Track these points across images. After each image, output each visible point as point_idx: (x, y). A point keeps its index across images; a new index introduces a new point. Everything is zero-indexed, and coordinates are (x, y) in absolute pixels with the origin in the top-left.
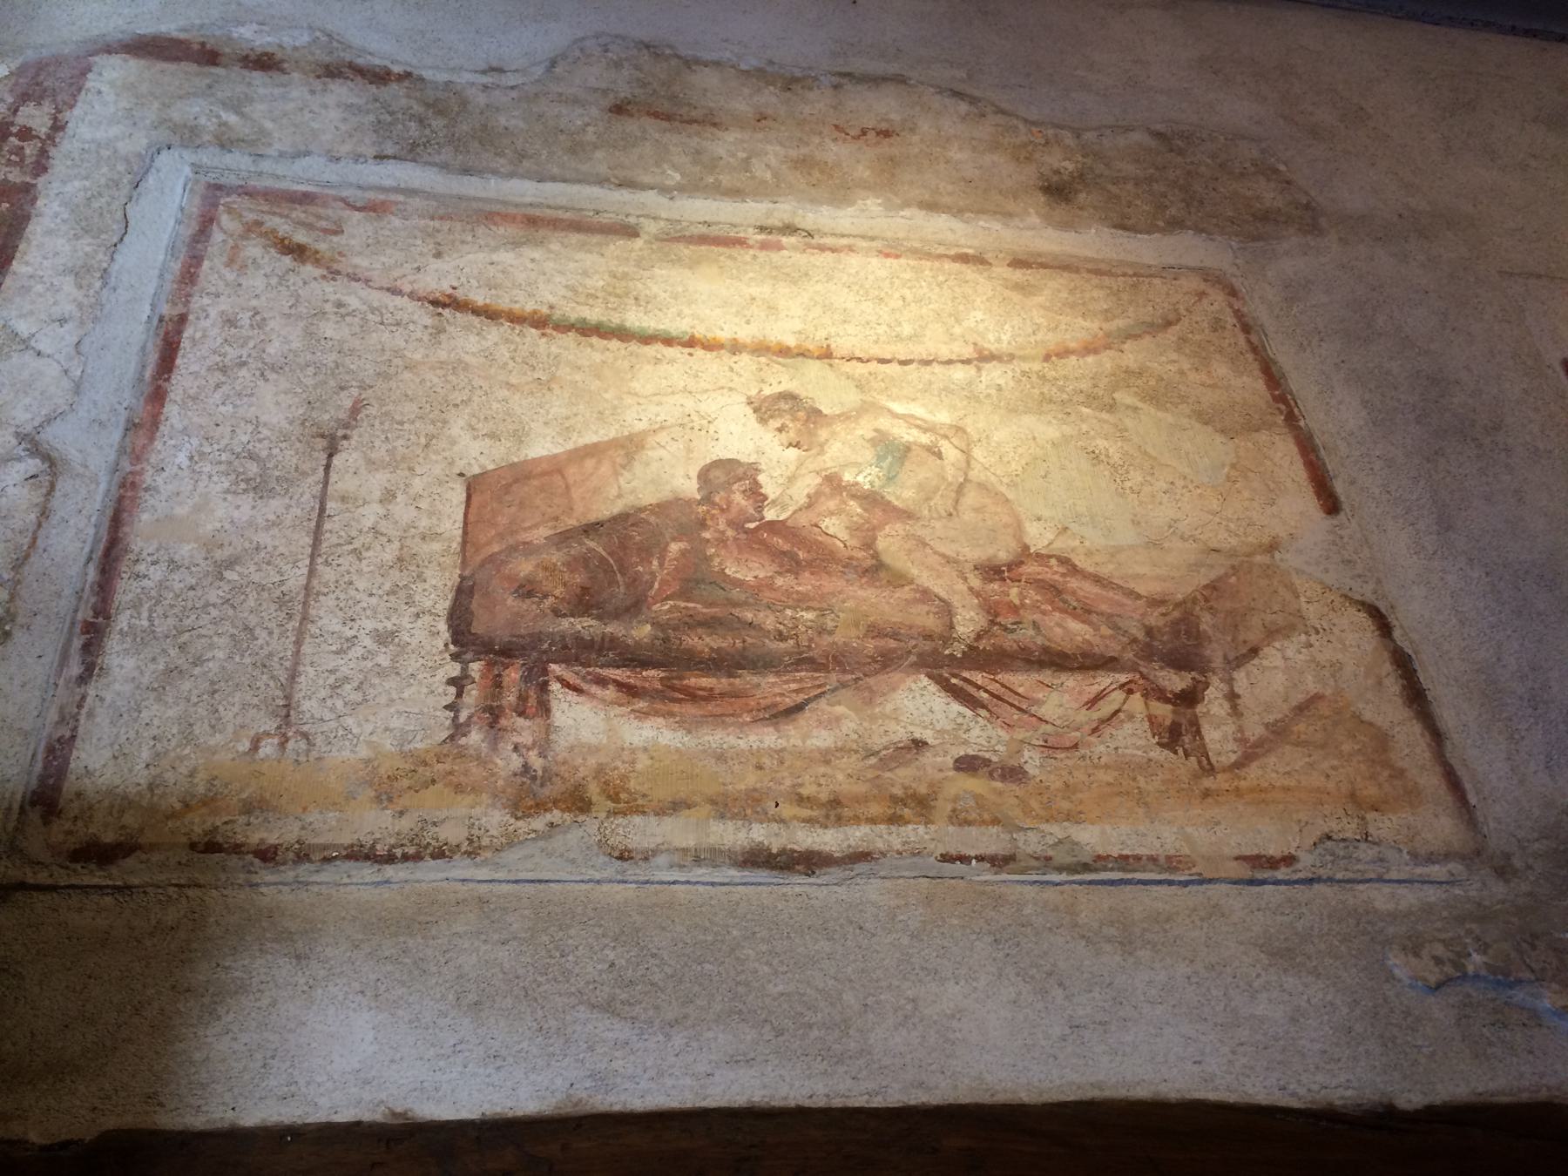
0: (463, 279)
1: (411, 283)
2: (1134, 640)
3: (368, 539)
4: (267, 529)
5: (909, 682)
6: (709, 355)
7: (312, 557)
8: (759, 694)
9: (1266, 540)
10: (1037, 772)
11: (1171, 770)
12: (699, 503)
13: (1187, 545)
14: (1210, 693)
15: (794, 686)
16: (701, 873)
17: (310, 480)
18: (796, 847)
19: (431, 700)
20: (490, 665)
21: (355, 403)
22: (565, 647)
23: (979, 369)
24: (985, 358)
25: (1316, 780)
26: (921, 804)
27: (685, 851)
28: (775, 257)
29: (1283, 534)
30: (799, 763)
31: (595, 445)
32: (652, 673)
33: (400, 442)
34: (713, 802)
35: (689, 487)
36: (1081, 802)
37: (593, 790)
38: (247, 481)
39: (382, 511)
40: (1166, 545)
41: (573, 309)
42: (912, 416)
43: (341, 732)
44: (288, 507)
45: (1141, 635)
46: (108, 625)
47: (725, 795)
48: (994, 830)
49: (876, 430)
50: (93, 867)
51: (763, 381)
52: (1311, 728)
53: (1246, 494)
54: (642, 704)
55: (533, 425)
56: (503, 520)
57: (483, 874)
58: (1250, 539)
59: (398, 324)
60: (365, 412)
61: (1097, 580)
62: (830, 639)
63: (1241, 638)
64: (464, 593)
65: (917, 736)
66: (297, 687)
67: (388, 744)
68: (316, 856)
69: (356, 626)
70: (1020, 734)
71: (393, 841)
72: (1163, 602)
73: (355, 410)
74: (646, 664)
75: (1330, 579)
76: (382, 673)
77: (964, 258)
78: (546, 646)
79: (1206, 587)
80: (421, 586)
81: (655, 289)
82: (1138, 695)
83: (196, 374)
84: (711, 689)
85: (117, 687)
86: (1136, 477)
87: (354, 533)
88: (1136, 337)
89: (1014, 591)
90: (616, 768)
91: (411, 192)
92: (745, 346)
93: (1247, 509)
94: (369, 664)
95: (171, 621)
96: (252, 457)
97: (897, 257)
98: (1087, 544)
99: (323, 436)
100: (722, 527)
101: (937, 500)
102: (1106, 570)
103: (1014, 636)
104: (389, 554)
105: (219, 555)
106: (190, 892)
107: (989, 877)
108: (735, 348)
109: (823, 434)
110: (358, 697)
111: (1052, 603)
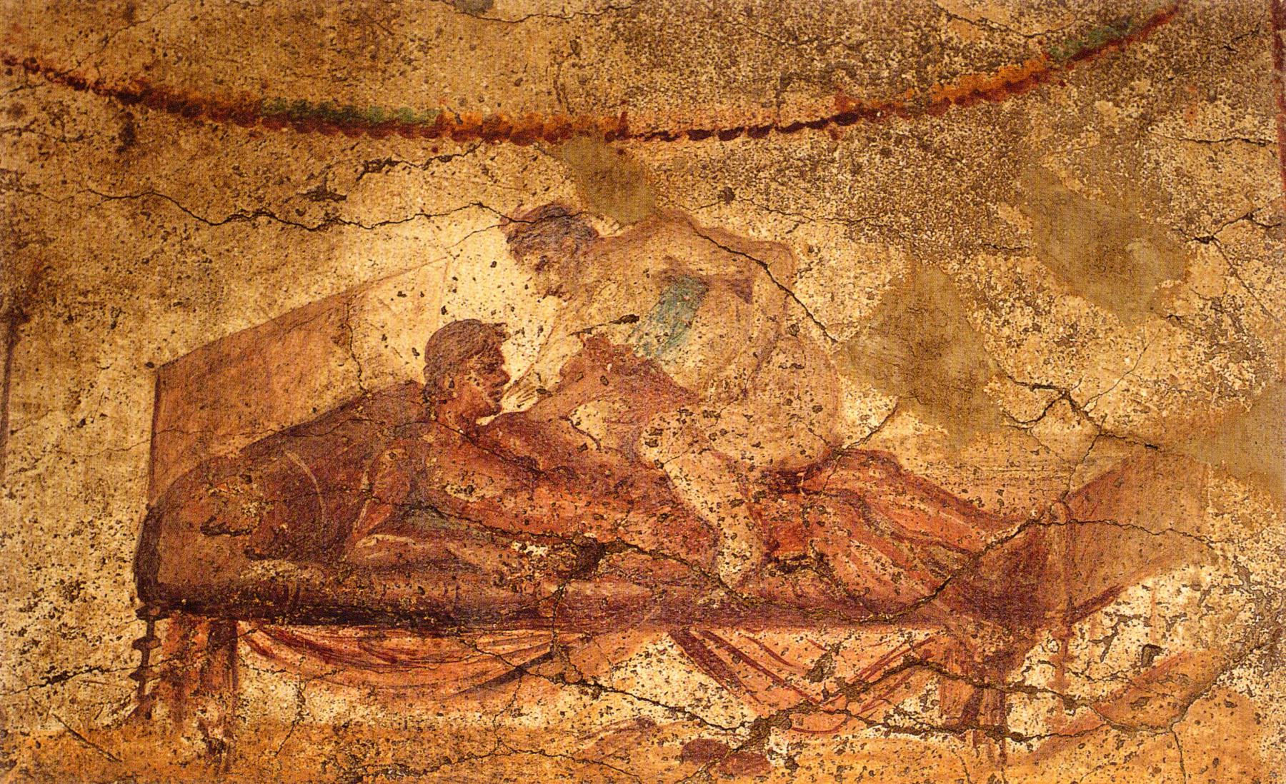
20: (179, 622)
23: (835, 136)
31: (303, 311)
32: (349, 632)
65: (645, 713)
80: (107, 522)
104: (72, 483)
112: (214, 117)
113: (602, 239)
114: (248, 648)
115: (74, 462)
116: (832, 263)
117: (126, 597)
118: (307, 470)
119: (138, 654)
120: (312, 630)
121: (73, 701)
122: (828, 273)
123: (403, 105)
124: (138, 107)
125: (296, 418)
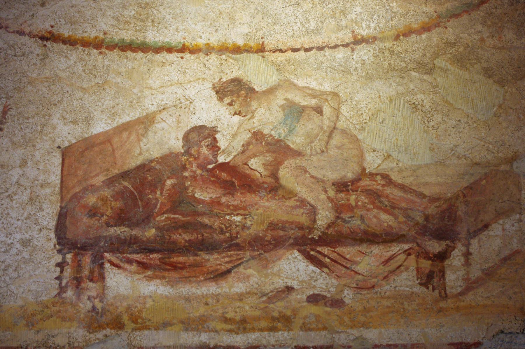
1: (29, 26)
2: (417, 224)
3: (14, 189)
5: (288, 255)
6: (193, 57)
8: (208, 265)
9: (510, 155)
10: (350, 301)
11: (424, 298)
13: (460, 162)
15: (227, 259)
18: (222, 344)
19: (49, 275)
20: (76, 255)
21: (5, 108)
22: (112, 244)
23: (353, 50)
24: (358, 41)
26: (286, 321)
33: (28, 130)
34: (182, 322)
35: (177, 144)
36: (371, 317)
37: (125, 318)
39: (21, 172)
41: (117, 33)
42: (308, 88)
43: (9, 293)
45: (421, 220)
48: (323, 333)
49: (286, 99)
52: (509, 271)
53: (504, 124)
54: (149, 273)
55: (95, 113)
56: (80, 173)
58: (500, 155)
59: (24, 55)
60: (9, 113)
61: (402, 187)
62: (248, 232)
64: (62, 216)
65: (289, 284)
67: (30, 298)
69: (12, 238)
70: (344, 281)
71: (35, 345)
72: (437, 199)
74: (151, 251)
76: (25, 262)
79: (466, 188)
81: (164, 13)
82: (413, 256)
84: (185, 263)
87: (8, 186)
88: (455, 16)
89: (353, 197)
90: (136, 307)
92: (213, 48)
93: (503, 135)
94: (20, 257)
98: (400, 165)
101: (316, 142)
103: (349, 225)
104: (25, 198)
108: (208, 50)
109: (254, 105)
110: (15, 275)
111: (373, 203)
113: (257, 92)
114: (109, 265)
115: (25, 189)
116: (356, 99)
118: (132, 189)
119: (58, 269)
120: (138, 256)
121: (29, 291)
122: (354, 103)
123: (167, 40)
124: (49, 42)
125: (126, 168)
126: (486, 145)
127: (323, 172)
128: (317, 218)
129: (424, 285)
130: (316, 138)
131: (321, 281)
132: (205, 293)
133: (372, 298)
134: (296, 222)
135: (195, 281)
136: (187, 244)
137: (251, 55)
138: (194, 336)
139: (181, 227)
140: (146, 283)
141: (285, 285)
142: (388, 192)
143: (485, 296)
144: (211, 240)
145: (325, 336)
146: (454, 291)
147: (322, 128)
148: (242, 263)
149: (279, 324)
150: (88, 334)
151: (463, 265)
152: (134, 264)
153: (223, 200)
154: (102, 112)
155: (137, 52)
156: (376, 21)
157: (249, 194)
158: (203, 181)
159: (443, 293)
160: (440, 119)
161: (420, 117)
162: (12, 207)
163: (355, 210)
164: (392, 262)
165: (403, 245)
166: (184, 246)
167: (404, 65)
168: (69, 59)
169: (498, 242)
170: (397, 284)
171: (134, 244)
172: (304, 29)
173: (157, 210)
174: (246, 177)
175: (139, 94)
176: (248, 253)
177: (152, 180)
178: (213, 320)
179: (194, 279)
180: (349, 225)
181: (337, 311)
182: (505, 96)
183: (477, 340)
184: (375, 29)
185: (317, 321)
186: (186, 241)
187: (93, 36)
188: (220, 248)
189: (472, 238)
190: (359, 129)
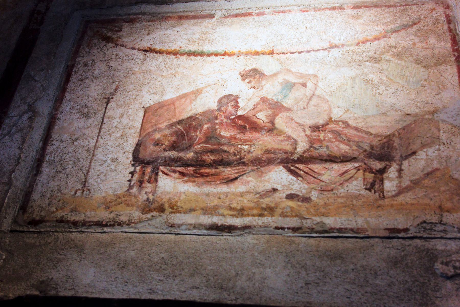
0: (155, 42)
1: (139, 45)
2: (365, 151)
3: (113, 130)
4: (87, 128)
6: (230, 58)
7: (98, 136)
8: (224, 174)
9: (432, 109)
11: (367, 198)
12: (216, 111)
13: (397, 113)
14: (392, 169)
15: (236, 171)
16: (195, 231)
17: (101, 113)
18: (226, 224)
19: (124, 179)
21: (117, 86)
22: (165, 161)
23: (329, 52)
25: (427, 201)
26: (271, 210)
27: (191, 224)
28: (261, 17)
29: (440, 106)
30: (233, 197)
32: (191, 168)
33: (128, 98)
35: (214, 105)
36: (330, 209)
37: (166, 205)
38: (84, 114)
39: (119, 121)
40: (388, 114)
42: (298, 73)
43: (98, 189)
44: (94, 121)
45: (367, 148)
46: (44, 159)
47: (207, 207)
49: (284, 79)
50: (33, 226)
51: (246, 65)
52: (430, 182)
53: (428, 91)
54: (186, 179)
55: (168, 89)
56: (153, 121)
57: (132, 230)
58: (425, 109)
60: (119, 89)
61: (356, 129)
62: (251, 155)
63: (410, 148)
64: (138, 145)
65: (275, 187)
66: (88, 175)
67: (110, 192)
68: (87, 225)
70: (312, 186)
71: (108, 220)
72: (381, 136)
73: (116, 89)
74: (189, 165)
75: (455, 123)
77: (334, 8)
78: (159, 161)
80: (126, 143)
82: (361, 171)
83: (74, 83)
84: (209, 173)
85: (44, 177)
86: (382, 88)
87: (110, 128)
89: (323, 134)
90: (174, 199)
91: (144, 14)
92: (243, 53)
94: (109, 168)
95: (59, 158)
96: (86, 106)
97: (307, 11)
98: (356, 115)
99: (106, 98)
100: (222, 119)
102: (360, 126)
103: (318, 151)
104: (119, 135)
105: (74, 137)
106: (55, 234)
107: (291, 234)
108: (239, 54)
109: (264, 82)
110: (104, 178)
111: (336, 138)
112: (167, 54)
114: (161, 173)
117: (129, 161)
118: (183, 130)
119: (130, 175)
120: (180, 168)
121: (111, 188)
123: (215, 50)
125: (181, 118)
126: (415, 103)
127: (304, 120)
128: (297, 146)
129: (369, 190)
130: (300, 101)
131: (296, 185)
132: (219, 192)
133: (331, 197)
134: (283, 149)
135: (214, 184)
136: (212, 162)
137: (265, 56)
138: (209, 218)
139: (209, 152)
140: (183, 184)
141: (272, 187)
142: (346, 131)
143: (412, 197)
144: (227, 160)
145: (297, 221)
146: (390, 194)
147: (305, 95)
148: (245, 173)
149: (266, 212)
150: (141, 215)
151: (397, 177)
152: (177, 173)
153: (238, 136)
154: (172, 88)
155: (197, 56)
156: (345, 36)
157: (254, 133)
158: (227, 125)
159: (381, 194)
160: (384, 88)
161: (370, 88)
162: (110, 140)
163: (323, 143)
164: (346, 174)
165: (355, 164)
166: (210, 163)
167: (361, 59)
168: (158, 61)
169: (423, 162)
170: (349, 188)
171: (179, 161)
172: (299, 42)
173: (196, 142)
174: (254, 123)
175: (195, 78)
176: (250, 168)
177: (195, 125)
178: (222, 208)
179: (214, 183)
180: (318, 151)
181: (306, 205)
182: (428, 74)
183: (405, 227)
184: (344, 40)
185: (292, 211)
186: (211, 160)
187: (173, 49)
188: (232, 164)
189: (403, 160)
190: (329, 95)
